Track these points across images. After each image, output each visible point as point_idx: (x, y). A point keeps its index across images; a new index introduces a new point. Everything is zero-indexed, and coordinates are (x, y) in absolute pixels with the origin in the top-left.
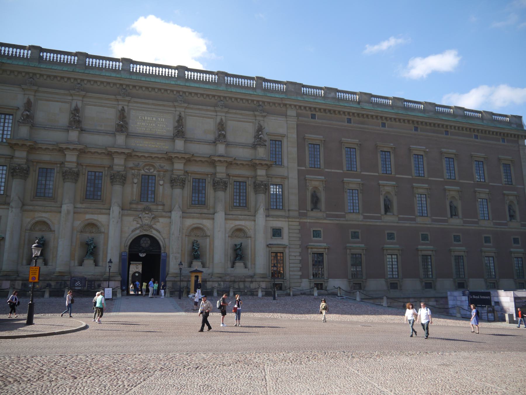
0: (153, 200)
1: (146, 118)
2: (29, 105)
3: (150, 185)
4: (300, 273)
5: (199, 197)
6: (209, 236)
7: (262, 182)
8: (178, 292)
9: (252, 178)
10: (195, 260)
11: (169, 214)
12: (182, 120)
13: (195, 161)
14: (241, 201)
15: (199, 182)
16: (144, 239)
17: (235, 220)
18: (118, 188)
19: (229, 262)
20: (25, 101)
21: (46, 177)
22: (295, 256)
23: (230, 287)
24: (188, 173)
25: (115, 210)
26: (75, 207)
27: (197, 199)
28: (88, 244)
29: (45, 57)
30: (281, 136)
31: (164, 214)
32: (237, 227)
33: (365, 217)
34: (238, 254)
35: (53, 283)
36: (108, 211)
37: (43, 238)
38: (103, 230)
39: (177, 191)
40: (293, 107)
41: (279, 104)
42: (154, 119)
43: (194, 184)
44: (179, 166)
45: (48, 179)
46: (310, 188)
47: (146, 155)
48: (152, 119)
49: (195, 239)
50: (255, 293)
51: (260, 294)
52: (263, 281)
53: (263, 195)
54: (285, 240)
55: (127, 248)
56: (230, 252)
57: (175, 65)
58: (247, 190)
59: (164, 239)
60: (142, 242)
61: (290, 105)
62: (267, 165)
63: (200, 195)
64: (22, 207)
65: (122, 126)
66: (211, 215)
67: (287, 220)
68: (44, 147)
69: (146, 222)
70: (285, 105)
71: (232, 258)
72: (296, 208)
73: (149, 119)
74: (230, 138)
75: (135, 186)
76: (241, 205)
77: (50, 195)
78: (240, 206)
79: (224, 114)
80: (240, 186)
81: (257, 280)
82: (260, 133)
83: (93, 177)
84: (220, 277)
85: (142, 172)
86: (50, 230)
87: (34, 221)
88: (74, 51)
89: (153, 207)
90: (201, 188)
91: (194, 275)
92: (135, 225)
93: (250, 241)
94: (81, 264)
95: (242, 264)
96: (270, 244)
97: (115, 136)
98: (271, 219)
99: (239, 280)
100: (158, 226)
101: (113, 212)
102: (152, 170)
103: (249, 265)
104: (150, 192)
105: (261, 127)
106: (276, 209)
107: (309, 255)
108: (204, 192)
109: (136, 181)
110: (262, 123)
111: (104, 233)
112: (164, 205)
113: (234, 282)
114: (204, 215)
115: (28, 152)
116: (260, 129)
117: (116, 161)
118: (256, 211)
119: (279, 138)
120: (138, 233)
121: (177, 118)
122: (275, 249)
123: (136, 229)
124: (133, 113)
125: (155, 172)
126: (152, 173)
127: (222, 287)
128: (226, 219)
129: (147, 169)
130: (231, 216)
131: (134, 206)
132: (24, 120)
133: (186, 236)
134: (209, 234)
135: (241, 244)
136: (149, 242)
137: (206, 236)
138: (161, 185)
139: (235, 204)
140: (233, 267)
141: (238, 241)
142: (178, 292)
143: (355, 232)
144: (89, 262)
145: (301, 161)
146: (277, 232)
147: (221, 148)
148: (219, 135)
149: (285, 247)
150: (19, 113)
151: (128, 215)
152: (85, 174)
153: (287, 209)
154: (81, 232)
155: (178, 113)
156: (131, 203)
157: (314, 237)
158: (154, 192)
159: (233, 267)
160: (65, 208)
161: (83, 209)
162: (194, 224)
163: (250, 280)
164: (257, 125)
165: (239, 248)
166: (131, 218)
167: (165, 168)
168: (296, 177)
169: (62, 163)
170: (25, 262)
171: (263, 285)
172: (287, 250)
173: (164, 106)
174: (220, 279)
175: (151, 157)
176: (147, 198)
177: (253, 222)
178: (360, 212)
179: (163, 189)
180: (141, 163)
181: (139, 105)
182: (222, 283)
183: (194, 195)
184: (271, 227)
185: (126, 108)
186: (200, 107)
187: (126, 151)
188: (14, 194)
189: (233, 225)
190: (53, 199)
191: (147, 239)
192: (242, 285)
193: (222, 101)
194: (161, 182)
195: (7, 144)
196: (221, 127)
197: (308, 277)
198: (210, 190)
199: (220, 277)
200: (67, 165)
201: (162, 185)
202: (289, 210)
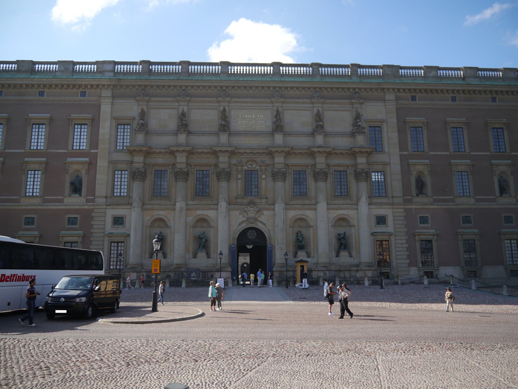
0: (256, 194)
1: (246, 116)
2: (143, 115)
3: (253, 179)
4: (408, 261)
5: (300, 189)
6: (312, 227)
7: (363, 170)
8: (285, 282)
9: (352, 166)
10: (299, 251)
11: (272, 207)
12: (279, 115)
13: (295, 153)
14: (343, 190)
15: (300, 174)
16: (250, 231)
17: (337, 209)
18: (224, 184)
19: (333, 251)
20: (140, 111)
21: (161, 178)
22: (402, 244)
23: (335, 277)
24: (289, 166)
25: (223, 205)
26: (187, 205)
27: (298, 191)
28: (200, 238)
29: (153, 69)
30: (381, 122)
31: (268, 206)
32: (340, 217)
33: (477, 200)
34: (343, 243)
35: (172, 275)
36: (216, 206)
37: (161, 233)
38: (212, 224)
39: (279, 184)
40: (391, 90)
41: (377, 89)
42: (254, 116)
43: (295, 176)
44: (279, 160)
45: (163, 179)
46: (414, 173)
47: (248, 151)
48: (252, 116)
49: (299, 229)
50: (361, 282)
51: (367, 283)
52: (369, 270)
53: (365, 183)
54: (390, 228)
55: (236, 241)
56: (334, 241)
57: (270, 62)
58: (348, 179)
59: (269, 231)
60: (248, 234)
61: (388, 89)
62: (367, 152)
63: (302, 187)
64: (142, 207)
65: (225, 126)
66: (313, 206)
67: (391, 207)
68: (158, 151)
69: (252, 215)
70: (383, 89)
71: (336, 247)
72: (401, 194)
73: (248, 116)
74: (328, 128)
75: (239, 181)
76: (343, 194)
77: (165, 194)
78: (341, 195)
79: (320, 105)
80: (340, 175)
81: (363, 269)
82: (358, 120)
83: (201, 176)
84: (325, 267)
85: (246, 167)
86: (167, 226)
87: (153, 219)
88: (178, 60)
89: (258, 201)
90: (302, 180)
91: (299, 264)
92: (241, 218)
93: (353, 229)
94: (195, 257)
95: (347, 253)
96: (374, 233)
97: (219, 136)
98: (374, 207)
99: (345, 269)
100: (263, 219)
101: (221, 207)
102: (254, 166)
103: (354, 253)
104: (253, 187)
105: (359, 114)
106: (379, 196)
107: (417, 242)
108: (305, 183)
109: (240, 176)
110: (359, 110)
111: (213, 227)
112: (267, 198)
113: (340, 271)
114: (306, 206)
115: (145, 157)
116: (358, 117)
117: (221, 159)
118: (358, 199)
119: (379, 124)
120: (244, 226)
121: (275, 114)
122: (380, 238)
123: (242, 222)
124: (233, 112)
125: (257, 167)
126: (254, 168)
127: (328, 276)
128: (328, 209)
129: (249, 165)
130: (333, 206)
131: (239, 200)
132: (140, 128)
133: (290, 227)
134: (312, 224)
135: (345, 233)
136: (255, 234)
137: (310, 226)
138: (263, 179)
139: (336, 194)
140: (337, 256)
141: (341, 230)
142: (285, 282)
143: (466, 217)
144: (202, 255)
145: (402, 146)
146: (381, 220)
147: (319, 139)
148: (317, 127)
149: (390, 234)
150: (135, 122)
151: (234, 210)
152: (194, 174)
153: (390, 195)
154: (194, 227)
155: (275, 108)
156: (236, 198)
157: (421, 223)
158: (257, 186)
159: (337, 256)
160: (178, 205)
161: (194, 206)
162: (296, 215)
163: (355, 269)
164: (355, 113)
165: (343, 238)
166: (237, 212)
167: (266, 162)
168: (399, 162)
169: (174, 165)
170: (147, 256)
171: (370, 274)
172: (393, 238)
173: (262, 102)
174: (325, 269)
175: (253, 153)
176: (252, 192)
177: (356, 211)
178: (472, 195)
179: (266, 183)
180: (243, 159)
181: (239, 104)
182: (327, 272)
183: (295, 187)
184: (375, 215)
185: (227, 108)
186: (297, 100)
187: (230, 149)
188: (135, 195)
189: (336, 215)
190: (168, 197)
191: (253, 231)
192: (347, 274)
193: (317, 92)
194: (264, 177)
195: (127, 151)
196: (319, 118)
197: (416, 265)
198: (310, 181)
199: (325, 267)
200: (178, 166)
202: (392, 197)
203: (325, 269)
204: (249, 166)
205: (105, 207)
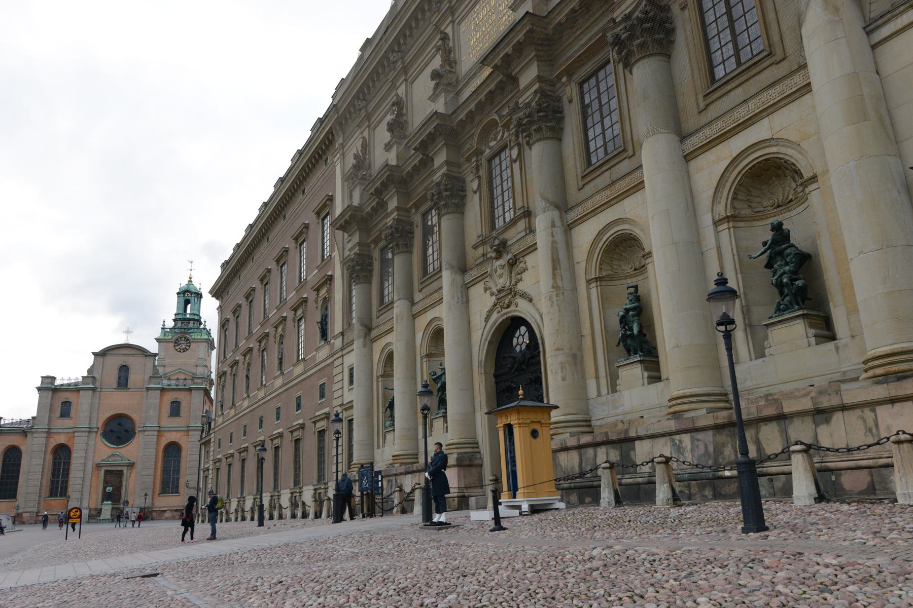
26: (413, 303)
69: (503, 281)
81: (848, 399)
123: (490, 313)
133: (589, 282)
151: (475, 282)
182: (686, 439)
201: (519, 154)
203: (672, 425)
204: (492, 144)
205: (340, 354)
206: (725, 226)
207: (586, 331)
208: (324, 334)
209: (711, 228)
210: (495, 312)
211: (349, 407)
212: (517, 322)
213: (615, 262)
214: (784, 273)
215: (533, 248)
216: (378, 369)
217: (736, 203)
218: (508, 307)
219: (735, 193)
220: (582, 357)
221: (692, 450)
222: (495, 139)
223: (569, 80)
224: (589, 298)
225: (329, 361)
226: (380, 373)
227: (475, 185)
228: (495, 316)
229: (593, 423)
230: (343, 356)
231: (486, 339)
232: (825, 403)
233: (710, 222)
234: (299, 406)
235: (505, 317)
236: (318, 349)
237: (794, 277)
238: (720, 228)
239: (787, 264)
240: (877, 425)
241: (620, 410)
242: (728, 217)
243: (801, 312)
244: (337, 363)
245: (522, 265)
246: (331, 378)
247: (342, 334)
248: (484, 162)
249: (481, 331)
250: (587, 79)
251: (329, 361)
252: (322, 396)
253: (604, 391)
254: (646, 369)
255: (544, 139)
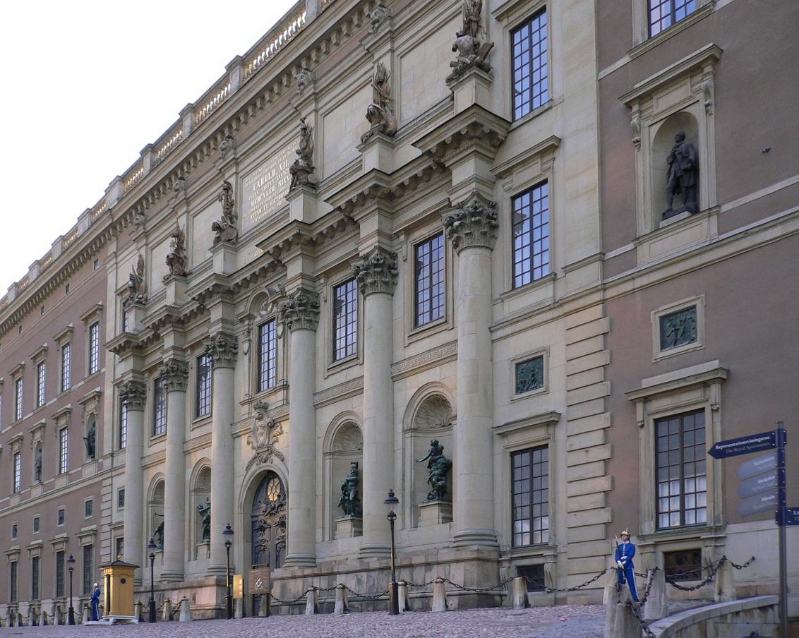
51: (437, 604)
81: (440, 559)
120: (256, 469)
133: (325, 454)
154: (196, 490)
182: (364, 575)
201: (284, 332)
205: (109, 475)
206: (409, 434)
207: (319, 492)
208: (91, 451)
209: (401, 434)
210: (255, 464)
211: (120, 526)
212: (270, 475)
213: (345, 441)
214: (434, 475)
215: (286, 418)
216: (148, 496)
217: (419, 419)
218: (265, 461)
219: (418, 412)
220: (315, 511)
221: (367, 582)
222: (266, 310)
223: (326, 283)
224: (324, 466)
225: (97, 480)
226: (150, 500)
227: (246, 347)
228: (254, 467)
229: (318, 561)
230: (112, 477)
231: (246, 485)
232: (431, 560)
233: (401, 430)
234: (61, 520)
235: (262, 469)
236: (84, 465)
237: (439, 478)
238: (407, 435)
239: (437, 469)
240: (449, 574)
241: (335, 553)
242: (411, 429)
243: (437, 502)
244: (105, 483)
245: (278, 429)
246: (99, 497)
247: (112, 455)
248: (256, 329)
249: (243, 479)
250: (340, 286)
251: (97, 480)
252: (89, 512)
253: (327, 538)
254: (354, 526)
255: (302, 329)
